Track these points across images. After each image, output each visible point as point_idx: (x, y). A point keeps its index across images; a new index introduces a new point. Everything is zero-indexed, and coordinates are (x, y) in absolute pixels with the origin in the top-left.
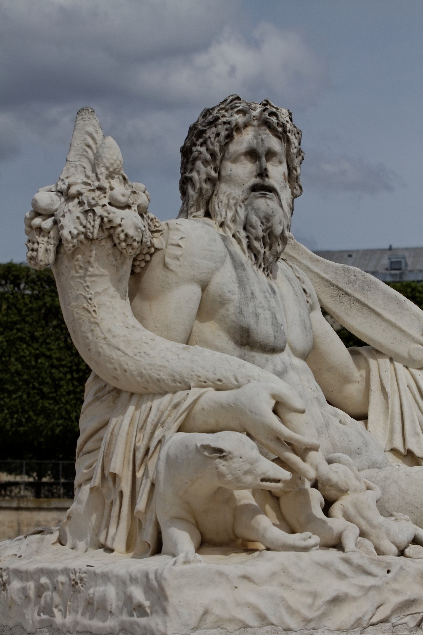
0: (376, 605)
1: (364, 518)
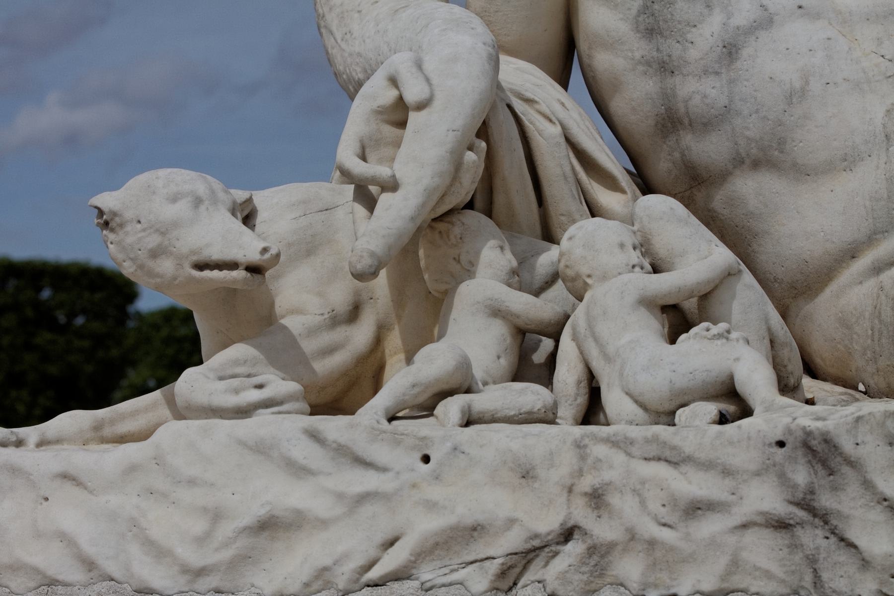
0: (380, 537)
1: (596, 340)
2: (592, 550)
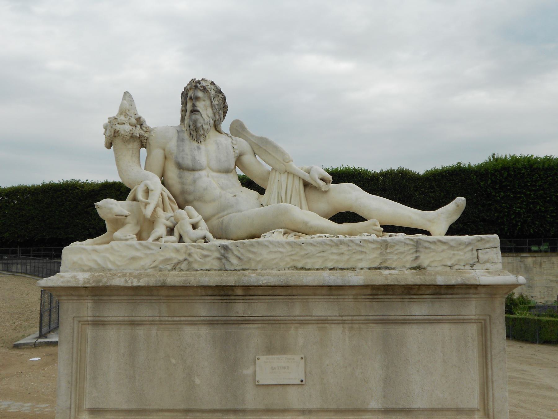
2: (189, 262)
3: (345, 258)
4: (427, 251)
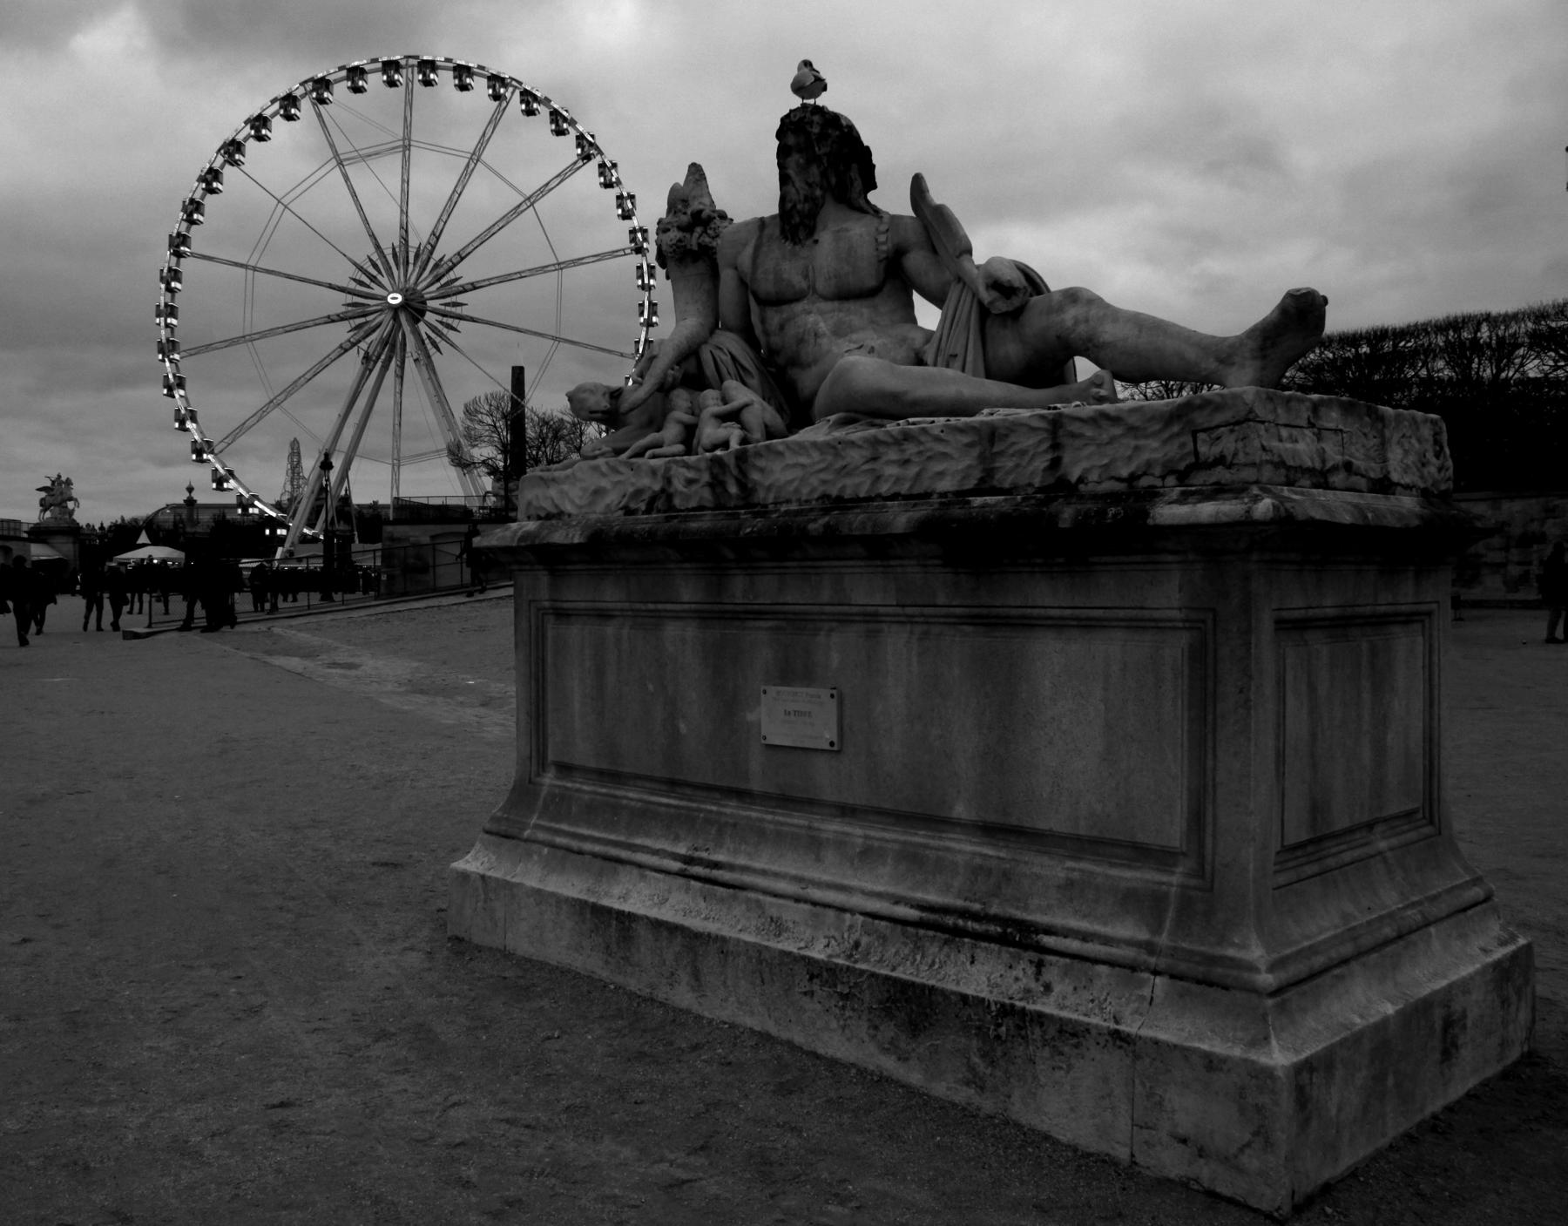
3: (912, 470)
4: (1078, 443)
